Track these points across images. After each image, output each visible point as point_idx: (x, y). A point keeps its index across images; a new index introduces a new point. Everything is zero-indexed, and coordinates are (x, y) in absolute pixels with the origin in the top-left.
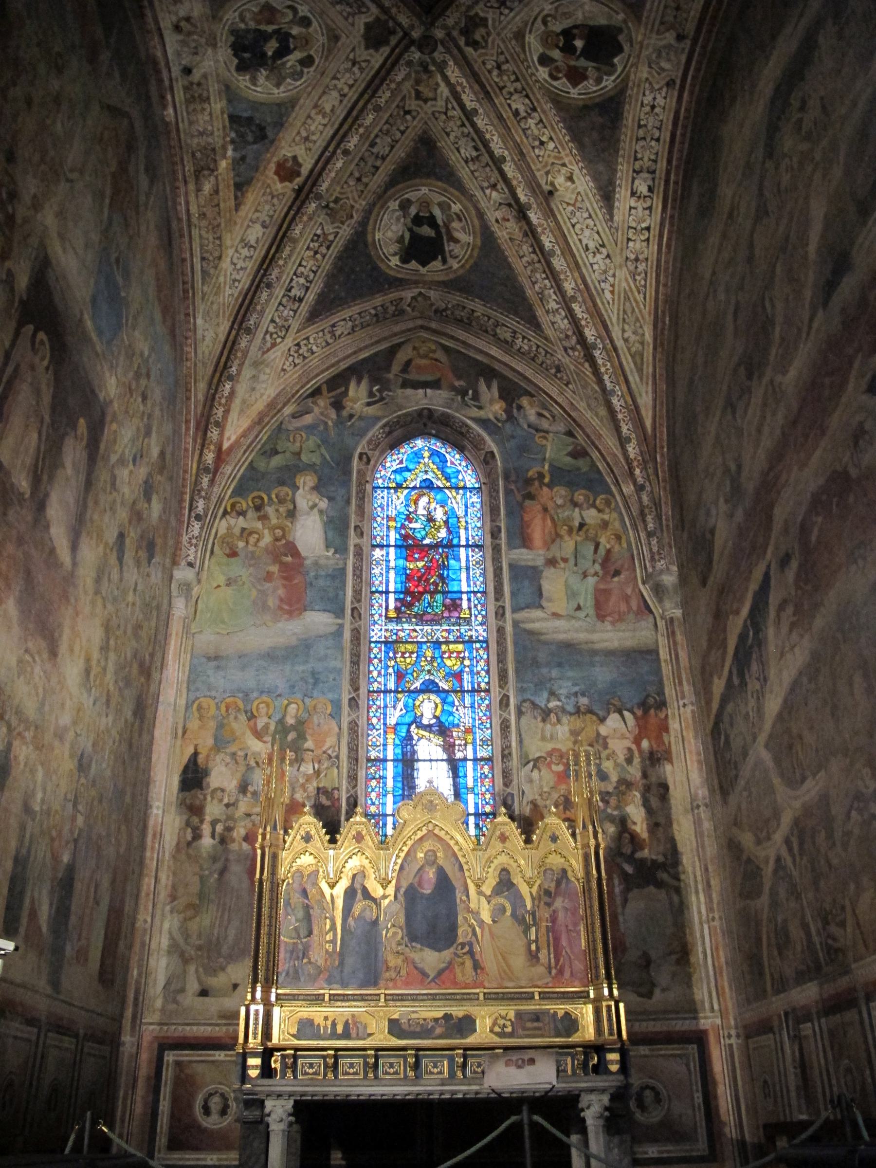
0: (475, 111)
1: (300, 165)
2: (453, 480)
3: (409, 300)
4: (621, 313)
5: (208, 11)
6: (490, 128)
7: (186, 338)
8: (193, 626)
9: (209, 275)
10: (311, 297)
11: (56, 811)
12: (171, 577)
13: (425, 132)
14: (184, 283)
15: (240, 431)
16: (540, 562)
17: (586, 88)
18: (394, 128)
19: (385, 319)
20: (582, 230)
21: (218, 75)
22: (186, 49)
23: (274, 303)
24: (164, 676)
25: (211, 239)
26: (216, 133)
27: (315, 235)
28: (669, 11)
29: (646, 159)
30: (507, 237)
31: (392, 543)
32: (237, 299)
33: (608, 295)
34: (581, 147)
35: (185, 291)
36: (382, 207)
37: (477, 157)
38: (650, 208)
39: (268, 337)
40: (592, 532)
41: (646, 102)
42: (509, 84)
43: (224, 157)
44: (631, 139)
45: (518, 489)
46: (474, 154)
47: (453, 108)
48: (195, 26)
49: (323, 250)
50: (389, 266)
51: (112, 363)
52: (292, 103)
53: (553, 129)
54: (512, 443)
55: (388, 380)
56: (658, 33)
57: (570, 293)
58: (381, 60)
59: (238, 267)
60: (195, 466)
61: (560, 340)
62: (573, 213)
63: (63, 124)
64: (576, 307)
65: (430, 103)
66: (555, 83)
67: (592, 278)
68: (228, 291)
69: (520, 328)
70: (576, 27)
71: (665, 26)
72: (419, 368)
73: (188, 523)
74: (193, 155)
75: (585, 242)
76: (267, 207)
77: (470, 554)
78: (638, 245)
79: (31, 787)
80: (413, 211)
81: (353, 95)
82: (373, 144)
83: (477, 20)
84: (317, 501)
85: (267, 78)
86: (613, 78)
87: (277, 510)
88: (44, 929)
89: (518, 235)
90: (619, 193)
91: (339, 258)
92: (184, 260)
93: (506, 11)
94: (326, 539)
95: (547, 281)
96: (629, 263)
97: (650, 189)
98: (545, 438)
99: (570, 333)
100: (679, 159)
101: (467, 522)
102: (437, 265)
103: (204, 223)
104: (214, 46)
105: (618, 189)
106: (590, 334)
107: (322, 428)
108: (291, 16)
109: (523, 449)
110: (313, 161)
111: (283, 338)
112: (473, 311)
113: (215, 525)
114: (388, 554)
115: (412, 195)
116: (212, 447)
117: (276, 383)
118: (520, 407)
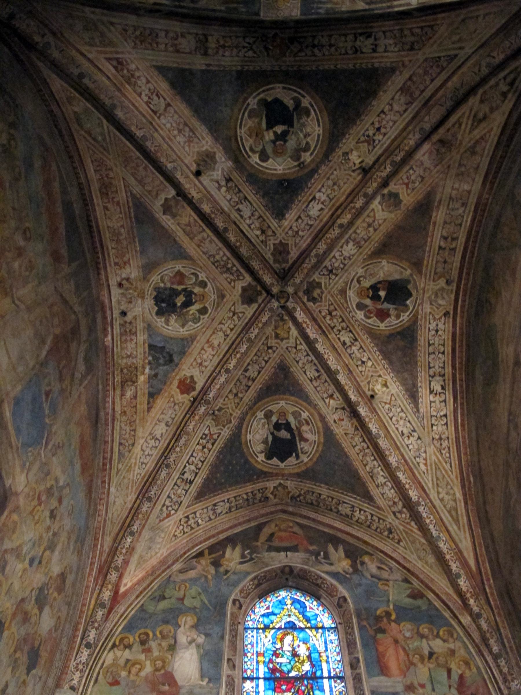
0: (316, 340)
1: (195, 383)
2: (313, 622)
3: (272, 489)
4: (435, 479)
5: (141, 274)
6: (327, 351)
7: (101, 500)
9: (124, 456)
10: (199, 481)
13: (282, 361)
14: (104, 458)
15: (135, 580)
16: (400, 688)
17: (390, 322)
18: (261, 359)
19: (254, 503)
20: (397, 421)
21: (143, 318)
22: (124, 299)
23: (171, 483)
25: (128, 431)
26: (139, 356)
27: (204, 434)
28: (439, 265)
29: (437, 367)
30: (343, 433)
31: (261, 675)
32: (143, 478)
33: (423, 467)
34: (391, 363)
35: (104, 465)
36: (253, 415)
37: (319, 376)
38: (445, 401)
39: (165, 508)
40: (442, 660)
41: (431, 328)
42: (337, 325)
43: (143, 373)
44: (425, 354)
45: (370, 626)
46: (317, 374)
47: (301, 343)
48: (132, 284)
49: (209, 445)
50: (257, 461)
51: (25, 465)
52: (192, 339)
53: (370, 352)
54: (359, 591)
55: (257, 546)
56: (434, 281)
57: (394, 464)
58: (251, 314)
59: (146, 453)
60: (93, 602)
61: (390, 507)
62: (390, 410)
63: (20, 267)
64: (400, 475)
65: (284, 341)
66: (369, 321)
67: (409, 455)
68: (137, 471)
69: (357, 502)
70: (380, 282)
71: (437, 276)
72: (281, 539)
73: (79, 650)
74: (122, 371)
75: (400, 429)
76: (170, 412)
77: (333, 685)
78: (440, 428)
80: (274, 419)
81: (232, 336)
82: (246, 370)
83: (315, 284)
84: (195, 636)
85: (176, 321)
86: (408, 313)
87: (160, 645)
89: (351, 430)
90: (422, 392)
91: (221, 452)
92: (106, 442)
93: (333, 277)
94: (202, 669)
95: (375, 462)
96: (435, 442)
97: (443, 388)
98: (386, 585)
99: (396, 500)
100: (461, 363)
101: (327, 657)
102: (292, 460)
103: (124, 418)
104: (143, 298)
105: (420, 390)
106: (414, 494)
107: (203, 580)
108: (194, 280)
109: (370, 593)
110: (204, 381)
111: (176, 511)
112: (320, 494)
113: (103, 656)
114: (257, 686)
115: (274, 408)
116: (110, 587)
117: (168, 546)
118: (363, 563)
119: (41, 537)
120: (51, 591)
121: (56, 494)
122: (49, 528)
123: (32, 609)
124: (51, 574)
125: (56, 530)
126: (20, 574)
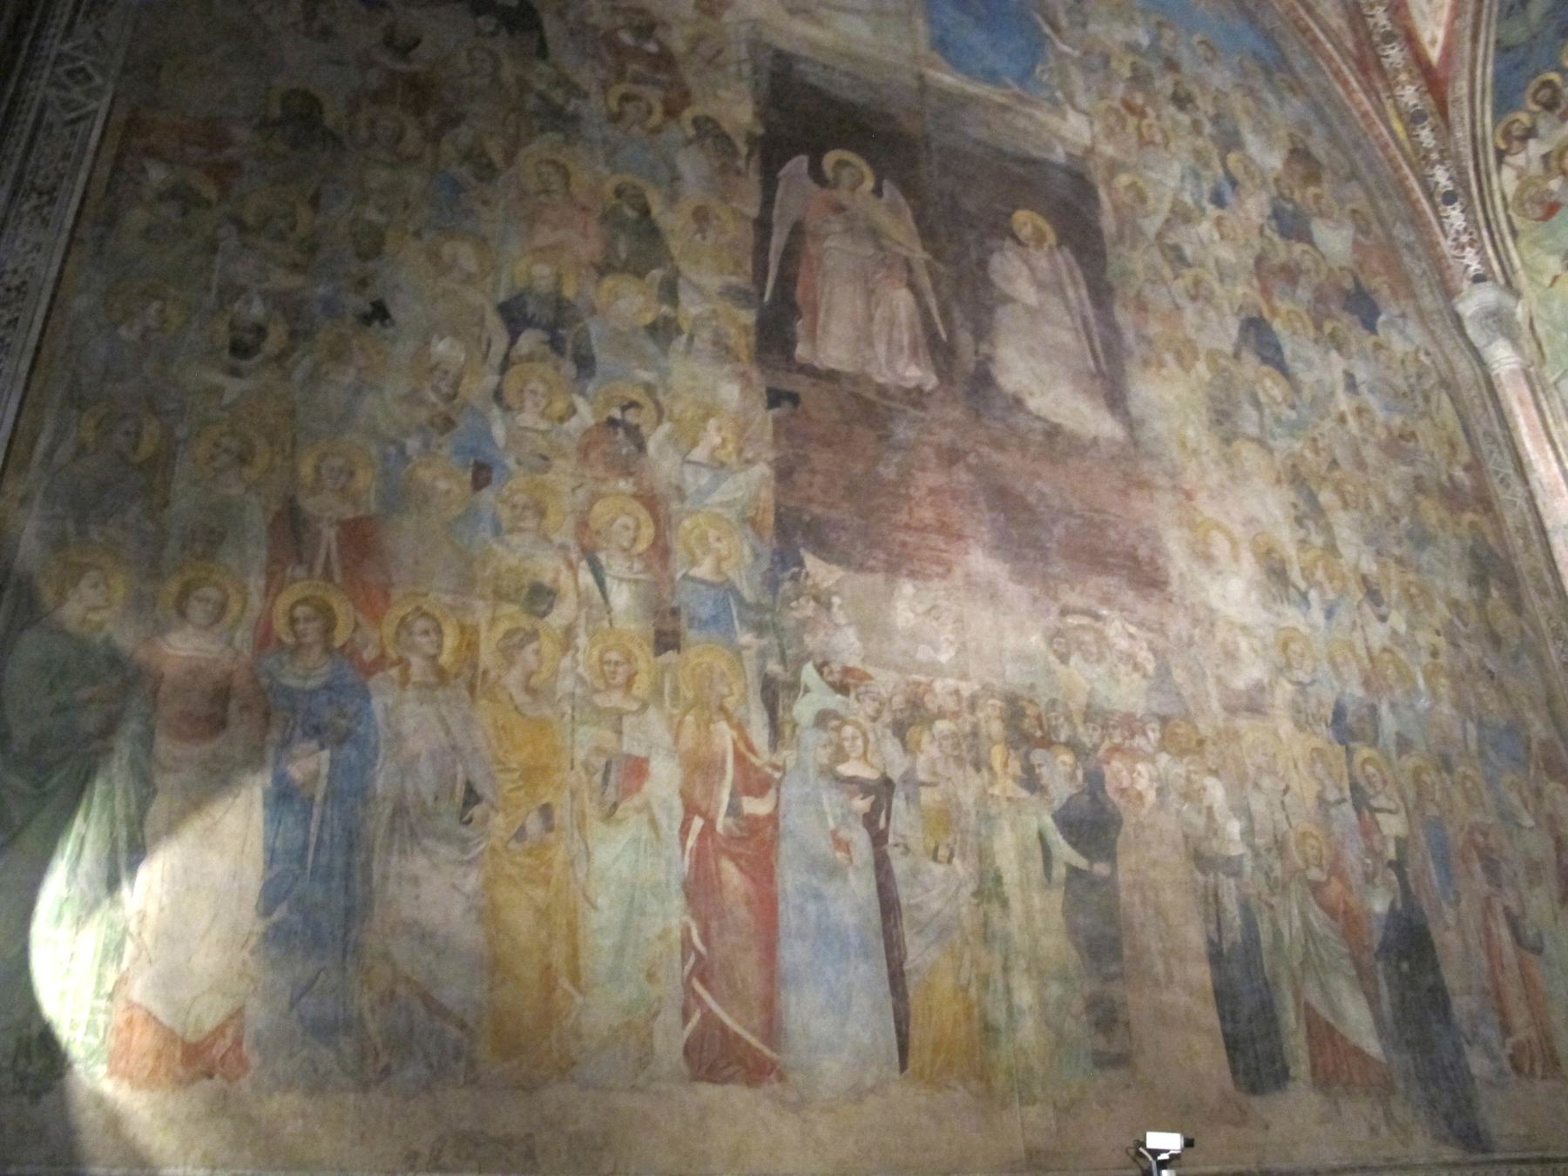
8: (1547, 374)
11: (1304, 835)
12: (1458, 320)
15: (1444, 15)
24: (1535, 485)
60: (1398, 126)
73: (1439, 218)
79: (1200, 822)
88: (1373, 1047)
113: (1495, 186)
116: (1403, 77)
119: (1198, 154)
120: (1297, 196)
121: (1154, 66)
122: (1196, 127)
123: (1289, 251)
124: (1271, 177)
125: (1211, 111)
126: (1216, 236)
